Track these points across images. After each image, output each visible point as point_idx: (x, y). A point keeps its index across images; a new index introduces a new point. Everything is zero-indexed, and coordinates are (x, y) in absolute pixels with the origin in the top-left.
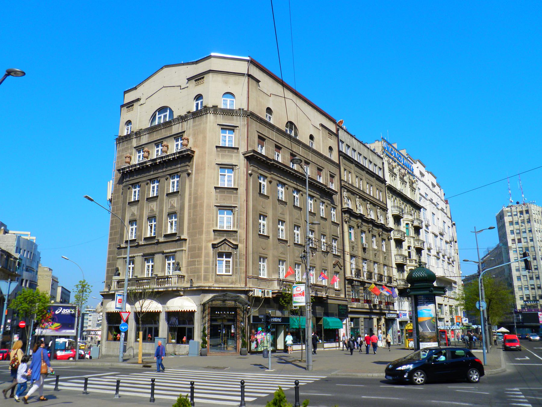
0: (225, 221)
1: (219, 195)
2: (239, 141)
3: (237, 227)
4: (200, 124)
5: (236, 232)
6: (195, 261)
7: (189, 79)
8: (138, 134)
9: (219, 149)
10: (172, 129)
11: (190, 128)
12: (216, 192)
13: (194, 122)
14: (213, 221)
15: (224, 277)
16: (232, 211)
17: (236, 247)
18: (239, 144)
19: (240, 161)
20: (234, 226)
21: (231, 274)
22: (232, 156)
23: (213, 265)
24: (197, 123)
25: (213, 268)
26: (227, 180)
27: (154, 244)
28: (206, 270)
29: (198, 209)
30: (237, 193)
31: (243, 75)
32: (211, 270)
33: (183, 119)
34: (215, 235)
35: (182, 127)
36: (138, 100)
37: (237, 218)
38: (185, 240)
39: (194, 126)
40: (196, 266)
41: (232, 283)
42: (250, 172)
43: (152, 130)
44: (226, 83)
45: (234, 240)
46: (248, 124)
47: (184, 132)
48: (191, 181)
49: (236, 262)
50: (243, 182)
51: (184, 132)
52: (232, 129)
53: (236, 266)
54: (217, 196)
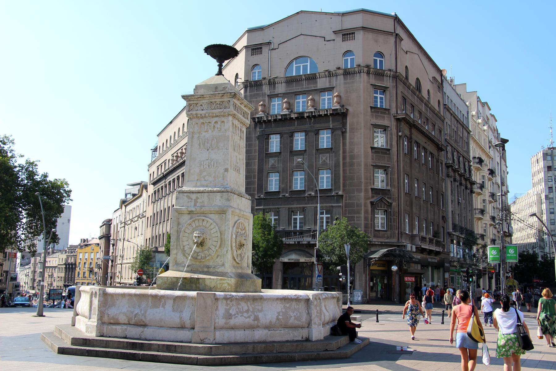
0: (380, 180)
1: (375, 155)
2: (390, 102)
4: (353, 82)
8: (272, 83)
9: (373, 110)
10: (316, 83)
12: (372, 152)
13: (345, 79)
14: (370, 180)
15: (381, 232)
16: (385, 170)
17: (390, 205)
18: (390, 106)
20: (387, 185)
21: (385, 229)
22: (384, 117)
23: (371, 221)
24: (348, 81)
25: (371, 224)
26: (380, 141)
28: (366, 226)
29: (355, 167)
30: (389, 154)
31: (390, 33)
32: (370, 225)
33: (330, 74)
34: (372, 193)
35: (330, 82)
36: (269, 43)
37: (391, 178)
38: (342, 196)
39: (345, 83)
40: (356, 222)
41: (388, 238)
42: (400, 134)
45: (388, 198)
46: (396, 85)
48: (344, 138)
49: (391, 219)
50: (395, 143)
52: (384, 90)
53: (391, 222)
54: (372, 156)
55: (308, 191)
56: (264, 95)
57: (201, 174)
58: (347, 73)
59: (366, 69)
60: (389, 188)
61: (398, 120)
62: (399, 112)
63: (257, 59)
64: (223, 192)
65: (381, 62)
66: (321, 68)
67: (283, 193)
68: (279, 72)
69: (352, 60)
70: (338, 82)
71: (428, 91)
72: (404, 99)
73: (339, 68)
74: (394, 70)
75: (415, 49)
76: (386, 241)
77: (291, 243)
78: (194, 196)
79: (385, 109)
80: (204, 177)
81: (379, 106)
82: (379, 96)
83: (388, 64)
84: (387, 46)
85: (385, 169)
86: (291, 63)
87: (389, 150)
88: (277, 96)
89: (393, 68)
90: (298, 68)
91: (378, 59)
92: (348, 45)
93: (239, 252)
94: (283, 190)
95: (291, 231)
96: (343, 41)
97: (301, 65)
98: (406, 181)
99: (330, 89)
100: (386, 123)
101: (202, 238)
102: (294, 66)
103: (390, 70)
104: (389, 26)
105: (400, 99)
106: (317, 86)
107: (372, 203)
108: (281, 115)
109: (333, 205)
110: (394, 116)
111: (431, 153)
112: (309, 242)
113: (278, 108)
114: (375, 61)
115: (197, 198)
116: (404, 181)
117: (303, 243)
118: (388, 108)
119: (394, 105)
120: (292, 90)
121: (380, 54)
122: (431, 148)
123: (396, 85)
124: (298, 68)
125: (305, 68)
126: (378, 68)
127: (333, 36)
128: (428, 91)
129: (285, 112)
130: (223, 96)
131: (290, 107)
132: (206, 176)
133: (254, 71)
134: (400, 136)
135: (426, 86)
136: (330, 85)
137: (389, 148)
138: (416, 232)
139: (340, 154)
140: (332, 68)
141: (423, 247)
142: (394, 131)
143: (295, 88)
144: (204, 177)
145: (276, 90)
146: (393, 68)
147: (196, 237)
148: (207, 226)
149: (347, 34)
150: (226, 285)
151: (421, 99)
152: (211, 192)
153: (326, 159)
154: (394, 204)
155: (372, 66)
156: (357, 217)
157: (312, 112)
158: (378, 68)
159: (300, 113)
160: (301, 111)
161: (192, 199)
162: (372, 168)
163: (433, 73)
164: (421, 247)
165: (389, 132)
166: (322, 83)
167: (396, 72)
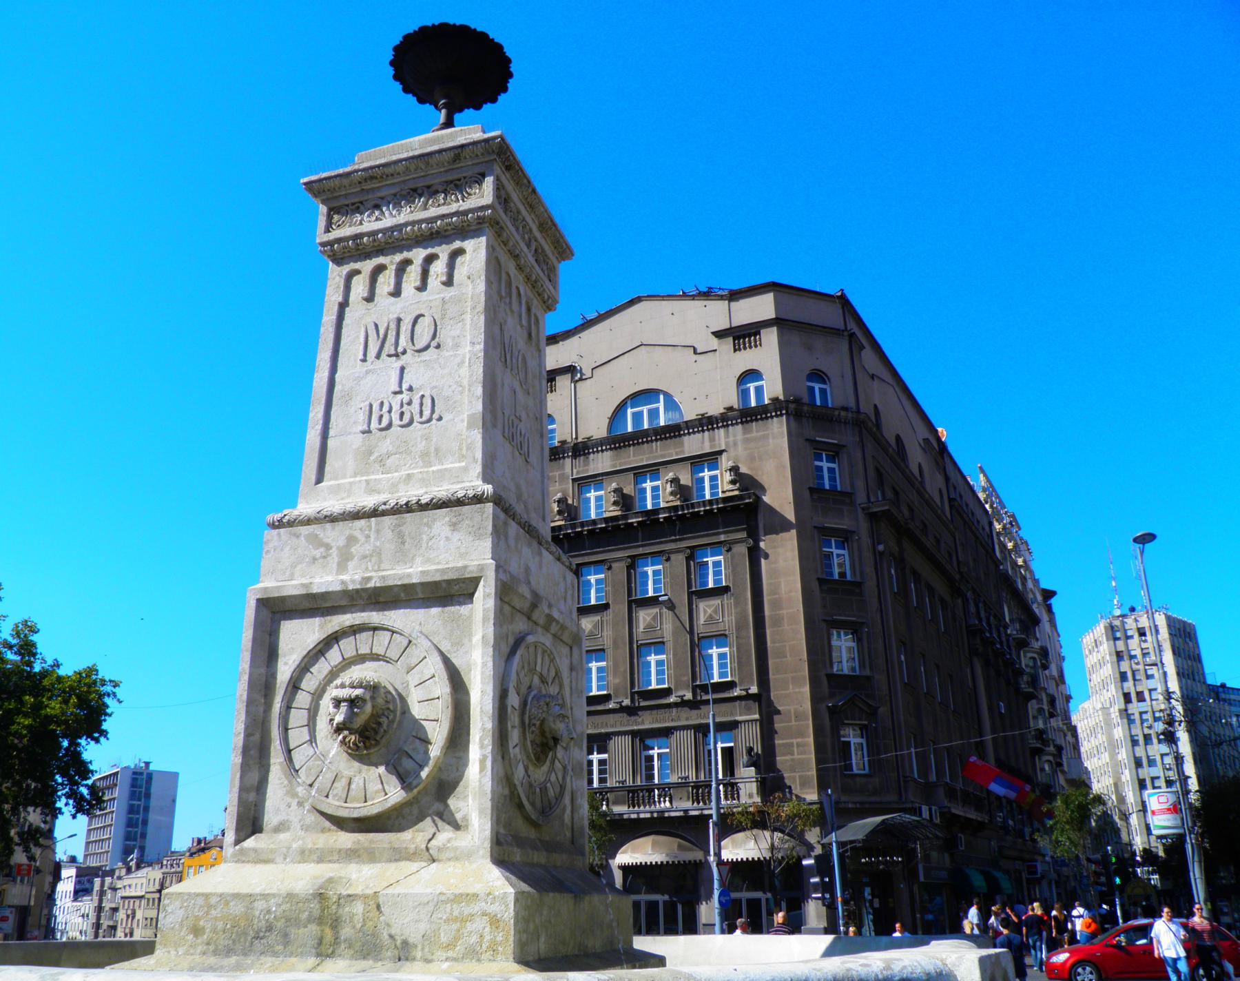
3: (871, 669)
4: (765, 437)
5: (868, 678)
6: (791, 745)
7: (719, 334)
8: (581, 449)
10: (682, 444)
11: (735, 444)
12: (822, 591)
13: (745, 432)
15: (858, 780)
17: (873, 713)
18: (852, 485)
19: (863, 526)
20: (862, 665)
21: (867, 771)
24: (754, 434)
27: (669, 706)
29: (786, 627)
31: (835, 332)
35: (712, 440)
36: (570, 370)
37: (869, 648)
39: (747, 441)
40: (796, 756)
42: (881, 548)
43: (617, 441)
44: (809, 348)
46: (862, 440)
47: (721, 452)
50: (869, 570)
51: (721, 452)
52: (835, 453)
55: (676, 690)
56: (563, 477)
57: (370, 453)
58: (747, 415)
59: (792, 406)
60: (867, 672)
61: (873, 517)
62: (873, 499)
64: (459, 502)
65: (823, 391)
66: (689, 414)
67: (616, 696)
68: (596, 427)
69: (759, 390)
70: (731, 439)
71: (920, 465)
72: (879, 474)
73: (730, 409)
74: (854, 409)
75: (887, 376)
76: (873, 799)
77: (642, 816)
78: (334, 535)
79: (842, 493)
80: (381, 461)
81: (827, 487)
82: (825, 465)
83: (837, 394)
84: (834, 360)
85: (854, 629)
86: (621, 408)
87: (859, 585)
88: (596, 480)
89: (852, 403)
90: (637, 417)
91: (817, 387)
92: (748, 359)
94: (616, 690)
95: (641, 789)
96: (735, 350)
97: (645, 409)
98: (903, 658)
99: (711, 459)
100: (844, 524)
101: (368, 708)
102: (629, 411)
103: (845, 409)
104: (832, 316)
105: (872, 473)
106: (683, 452)
107: (833, 711)
108: (606, 520)
109: (739, 718)
110: (863, 509)
111: (942, 600)
112: (686, 811)
113: (598, 505)
114: (812, 390)
115: (351, 540)
116: (899, 658)
117: (673, 814)
118: (849, 490)
119: (860, 484)
120: (625, 463)
121: (818, 375)
122: (941, 587)
123: (862, 440)
124: (637, 417)
125: (654, 414)
126: (818, 403)
127: (714, 343)
128: (920, 465)
129: (614, 511)
130: (457, 158)
131: (625, 501)
132: (389, 455)
134: (881, 554)
135: (916, 457)
136: (711, 447)
137: (858, 579)
138: (933, 777)
139: (746, 599)
140: (715, 408)
141: (954, 811)
142: (866, 540)
143: (636, 457)
144: (381, 461)
145: (592, 466)
146: (852, 404)
147: (337, 702)
148: (393, 653)
149: (743, 335)
150: (480, 924)
151: (909, 478)
152: (408, 508)
153: (716, 611)
154: (882, 710)
155: (806, 399)
156: (798, 745)
157: (675, 508)
158: (818, 403)
159: (647, 513)
160: (649, 507)
161: (328, 547)
162: (824, 625)
163: (923, 433)
164: (950, 812)
165: (855, 545)
166: (694, 444)
167: (858, 411)
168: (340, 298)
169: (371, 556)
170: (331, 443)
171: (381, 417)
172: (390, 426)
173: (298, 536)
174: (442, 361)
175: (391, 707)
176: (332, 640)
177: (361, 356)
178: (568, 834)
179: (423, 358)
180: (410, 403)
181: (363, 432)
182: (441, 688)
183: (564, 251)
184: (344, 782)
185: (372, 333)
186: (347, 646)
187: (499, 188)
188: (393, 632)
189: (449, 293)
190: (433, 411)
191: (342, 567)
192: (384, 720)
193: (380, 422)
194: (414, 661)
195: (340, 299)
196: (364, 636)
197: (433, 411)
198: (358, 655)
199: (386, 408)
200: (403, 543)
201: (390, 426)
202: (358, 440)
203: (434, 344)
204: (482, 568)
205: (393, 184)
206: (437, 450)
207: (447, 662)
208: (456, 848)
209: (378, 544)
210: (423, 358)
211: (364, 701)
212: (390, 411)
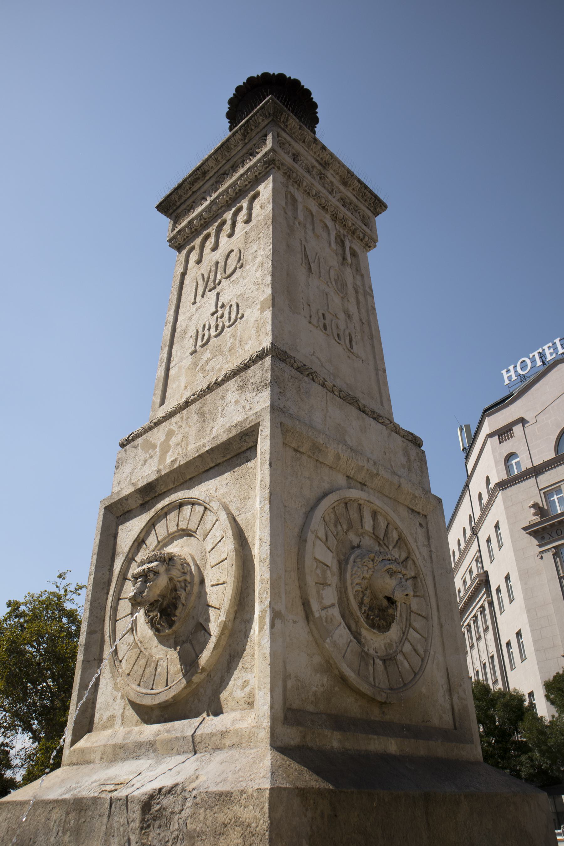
36: (522, 421)
63: (508, 446)
93: (376, 641)
133: (509, 464)
161: (154, 447)
168: (181, 270)
169: (182, 441)
170: (172, 372)
171: (204, 335)
172: (209, 339)
173: (136, 447)
174: (244, 274)
175: (188, 578)
176: (151, 525)
177: (193, 301)
178: (448, 718)
179: (231, 280)
180: (222, 316)
181: (191, 354)
182: (228, 547)
183: (378, 206)
184: (153, 665)
185: (200, 282)
186: (161, 530)
187: (277, 138)
188: (193, 504)
189: (249, 227)
190: (237, 313)
191: (162, 459)
192: (182, 594)
193: (202, 341)
194: (209, 526)
195: (182, 270)
196: (172, 516)
197: (237, 313)
198: (169, 535)
199: (207, 327)
200: (204, 421)
201: (209, 339)
202: (189, 360)
203: (239, 265)
204: (258, 414)
205: (211, 177)
206: (240, 341)
207: (233, 521)
208: (237, 732)
209: (187, 430)
210: (231, 280)
211: (157, 573)
212: (209, 329)
